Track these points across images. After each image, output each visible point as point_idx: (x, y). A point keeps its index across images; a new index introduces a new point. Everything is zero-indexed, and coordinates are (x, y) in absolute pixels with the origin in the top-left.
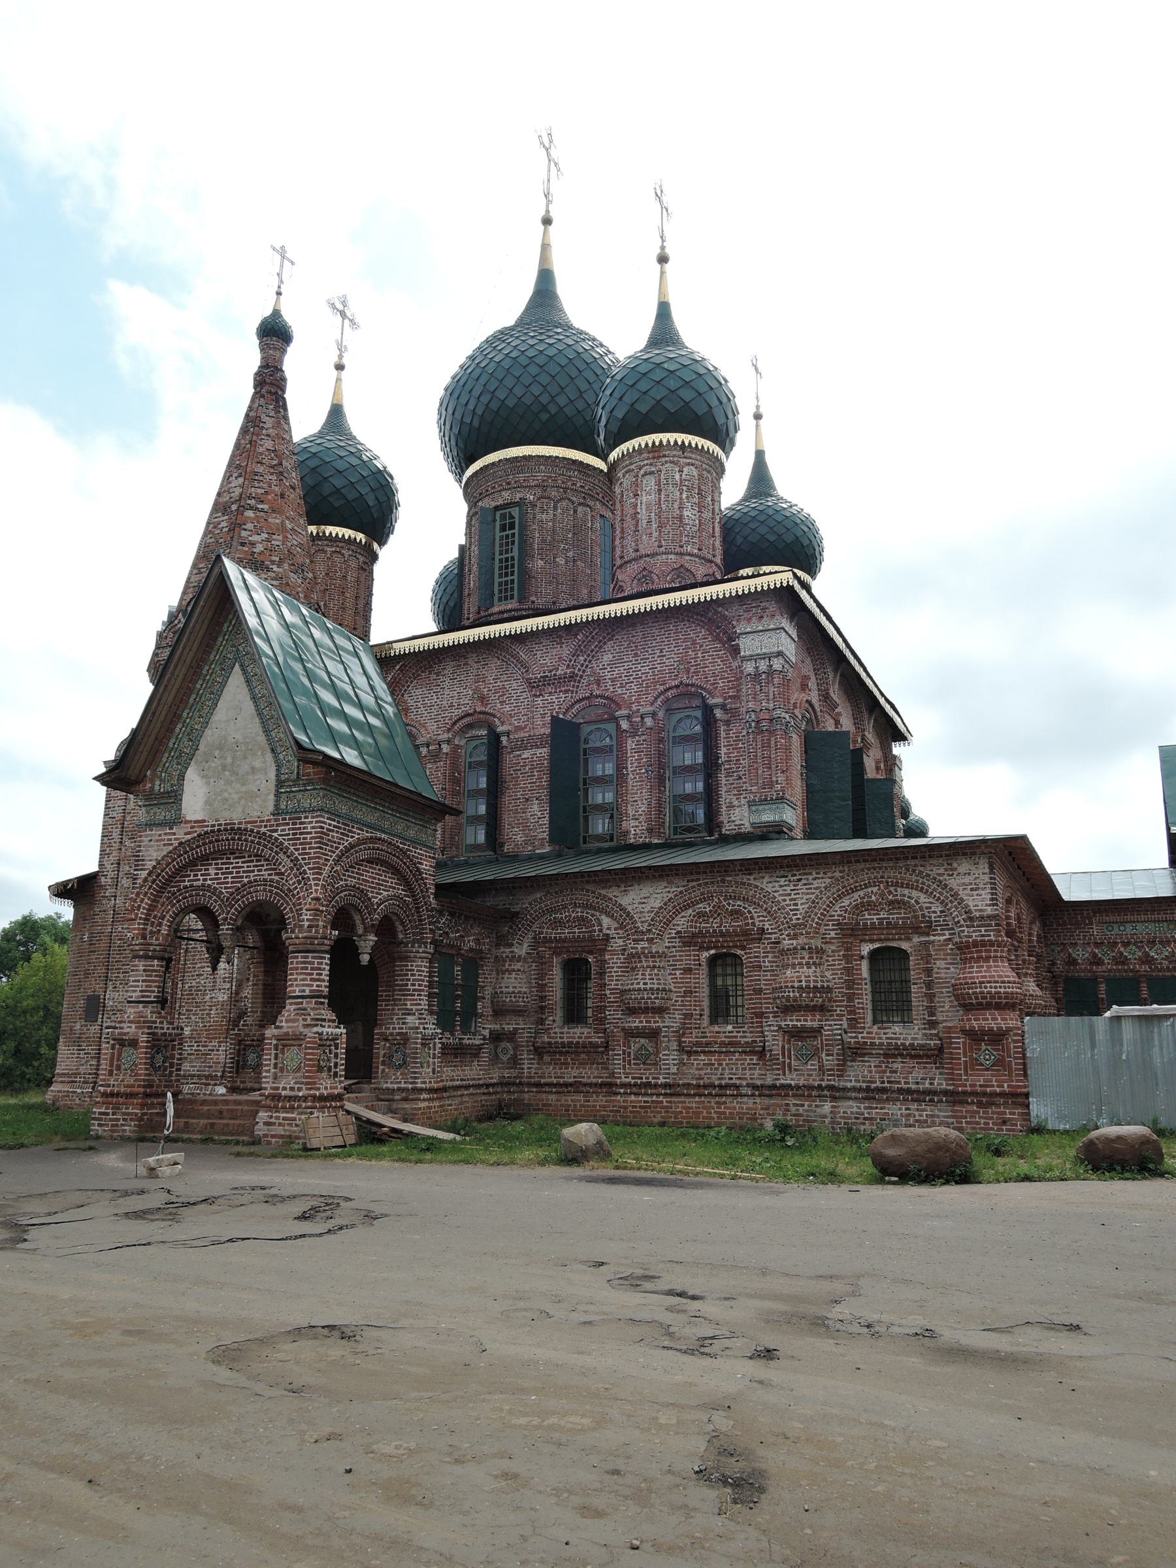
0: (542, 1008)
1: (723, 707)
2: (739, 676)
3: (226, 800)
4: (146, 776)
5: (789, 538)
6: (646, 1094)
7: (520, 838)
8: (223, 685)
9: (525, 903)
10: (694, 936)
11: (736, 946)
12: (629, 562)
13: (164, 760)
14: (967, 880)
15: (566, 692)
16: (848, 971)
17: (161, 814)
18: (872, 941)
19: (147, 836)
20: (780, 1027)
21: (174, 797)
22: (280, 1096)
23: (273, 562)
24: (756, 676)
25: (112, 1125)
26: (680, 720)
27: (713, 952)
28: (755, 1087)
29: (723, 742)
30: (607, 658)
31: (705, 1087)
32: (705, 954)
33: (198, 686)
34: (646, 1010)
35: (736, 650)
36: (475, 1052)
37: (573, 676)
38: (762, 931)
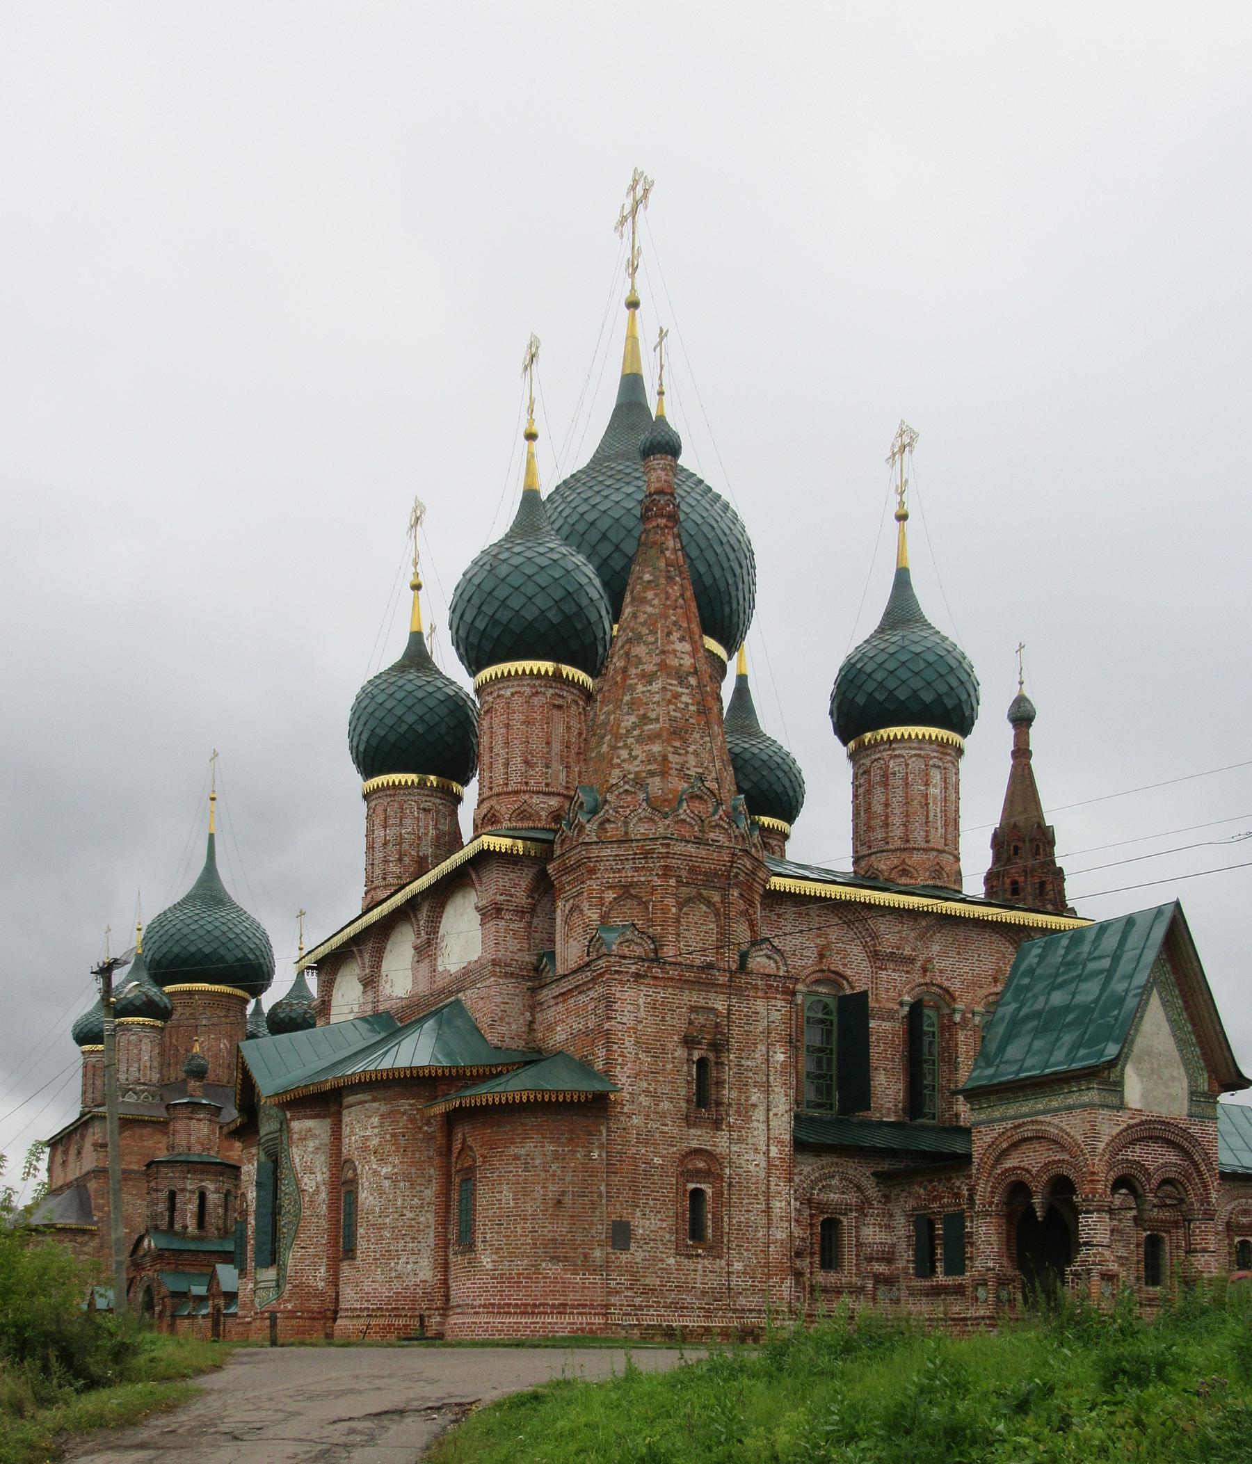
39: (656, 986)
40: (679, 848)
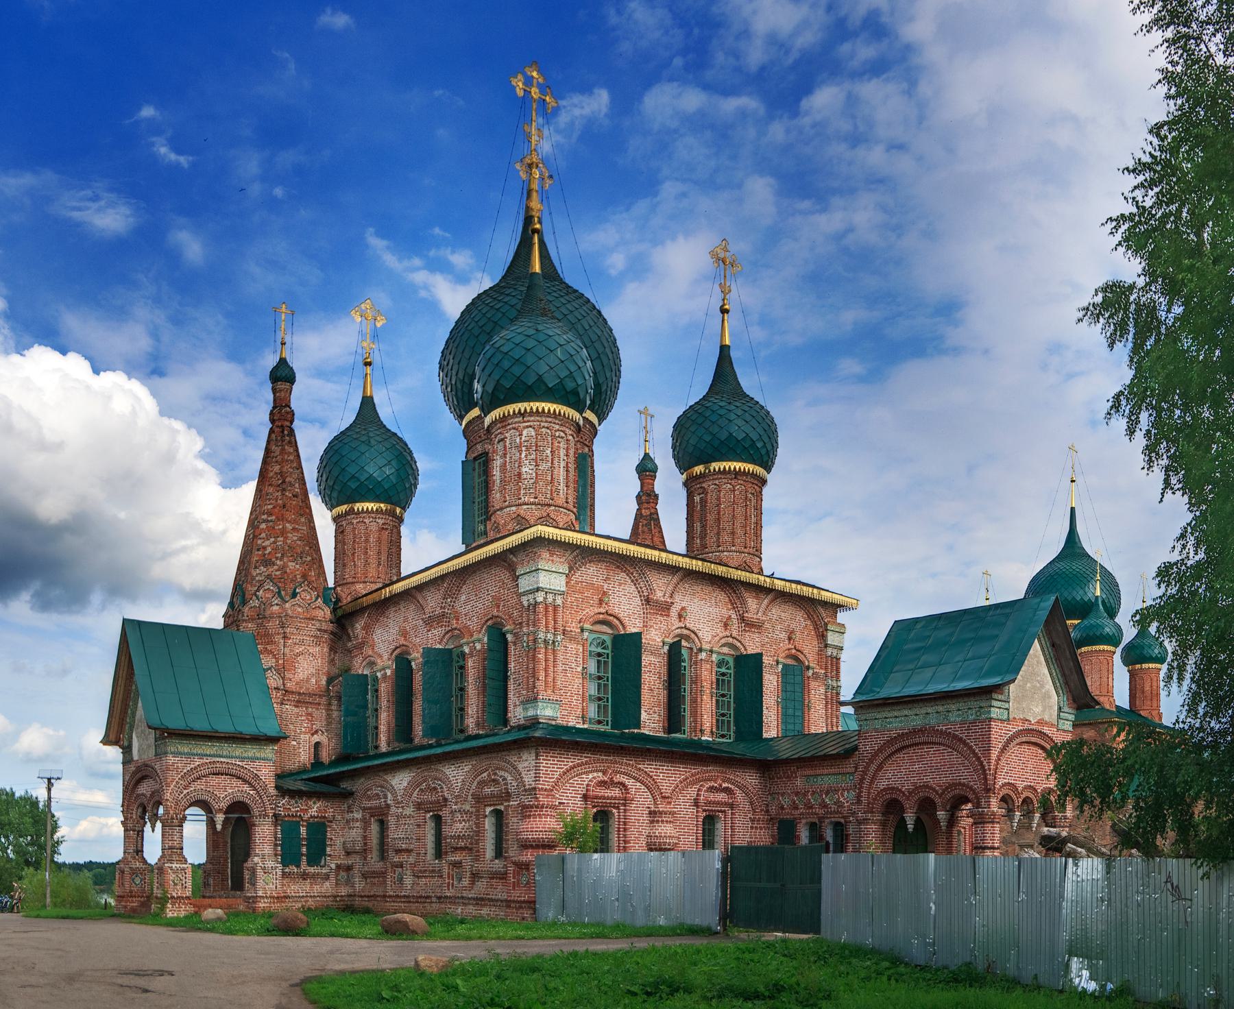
9: (358, 785)
10: (419, 804)
14: (526, 764)
16: (477, 825)
28: (440, 898)
30: (463, 597)
32: (428, 815)
36: (327, 877)
38: (446, 800)
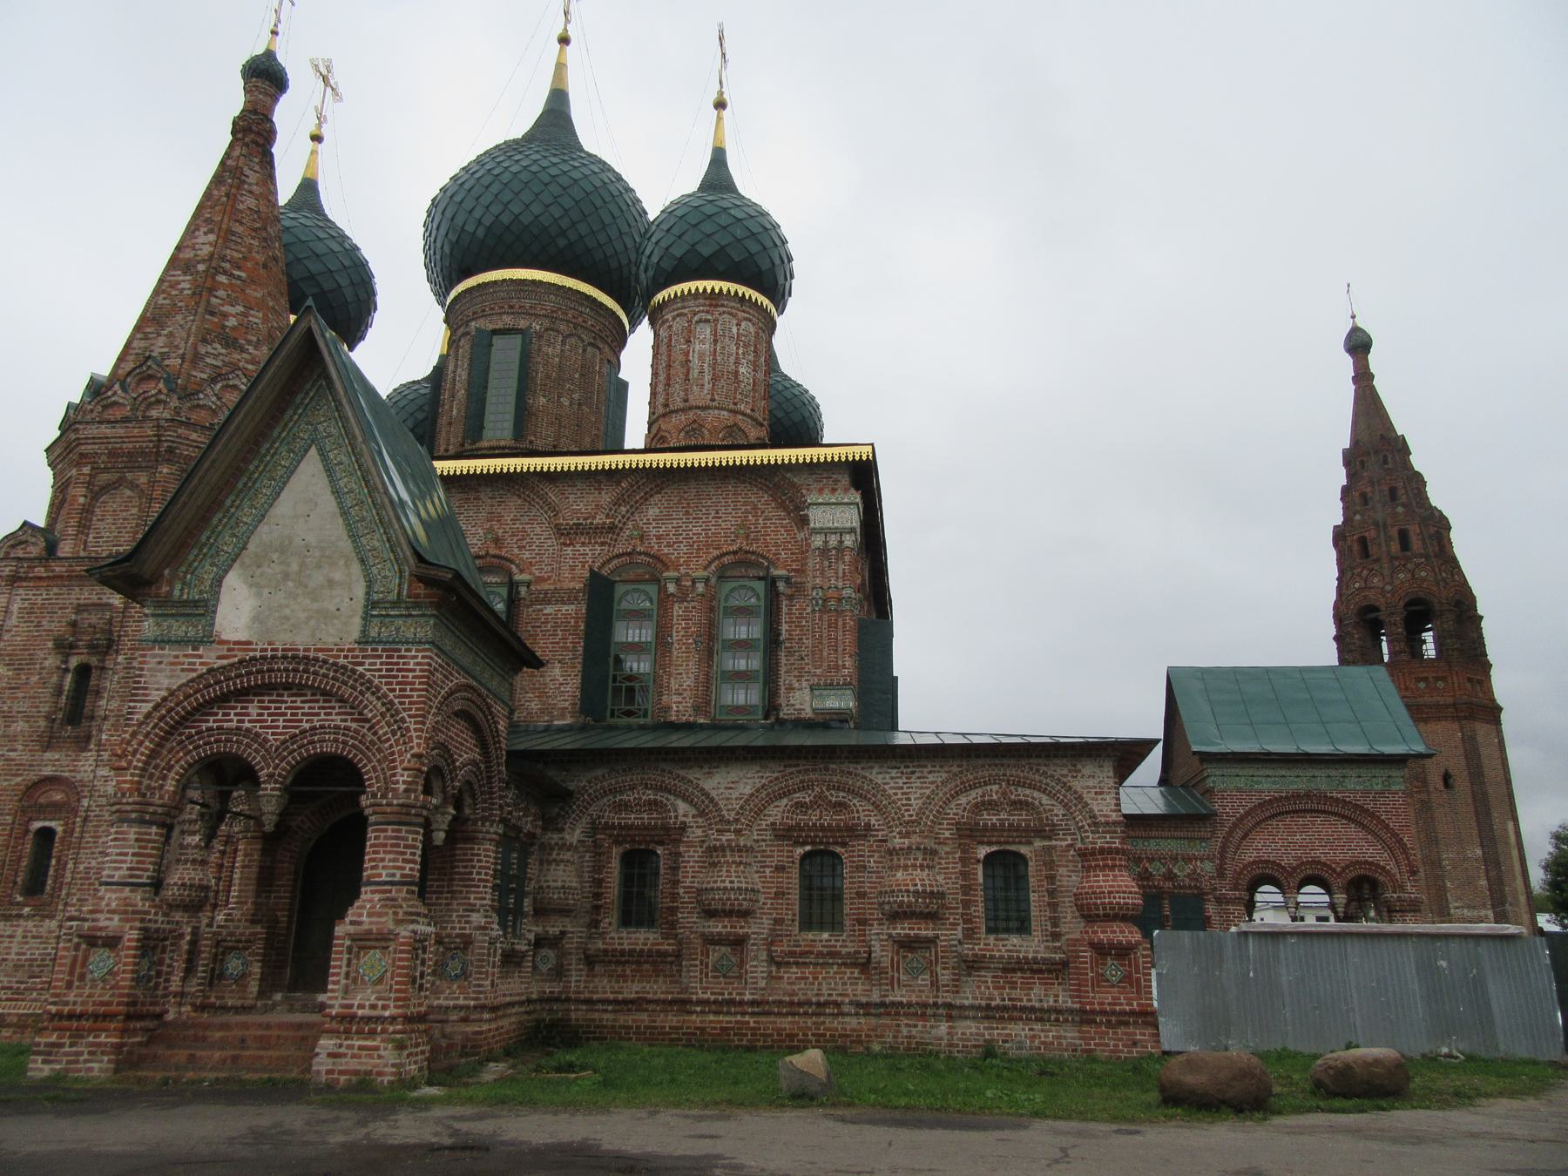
0: (597, 908)
1: (787, 580)
2: (804, 550)
3: (287, 618)
4: (162, 575)
5: (796, 417)
6: (728, 1013)
7: (534, 706)
8: (291, 471)
9: (578, 781)
10: (790, 828)
11: (836, 843)
12: (676, 411)
13: (191, 557)
15: (603, 544)
17: (179, 628)
18: (990, 843)
19: (155, 656)
20: (890, 936)
21: (204, 608)
22: (353, 1017)
23: (249, 342)
24: (824, 551)
25: (69, 1062)
26: (627, 593)
27: (808, 848)
28: (859, 1005)
29: (784, 618)
30: (653, 512)
31: (800, 1004)
32: (800, 851)
33: (252, 467)
34: (729, 914)
35: (804, 521)
37: (612, 528)
38: (868, 827)
39: (38, 588)
40: (93, 431)
